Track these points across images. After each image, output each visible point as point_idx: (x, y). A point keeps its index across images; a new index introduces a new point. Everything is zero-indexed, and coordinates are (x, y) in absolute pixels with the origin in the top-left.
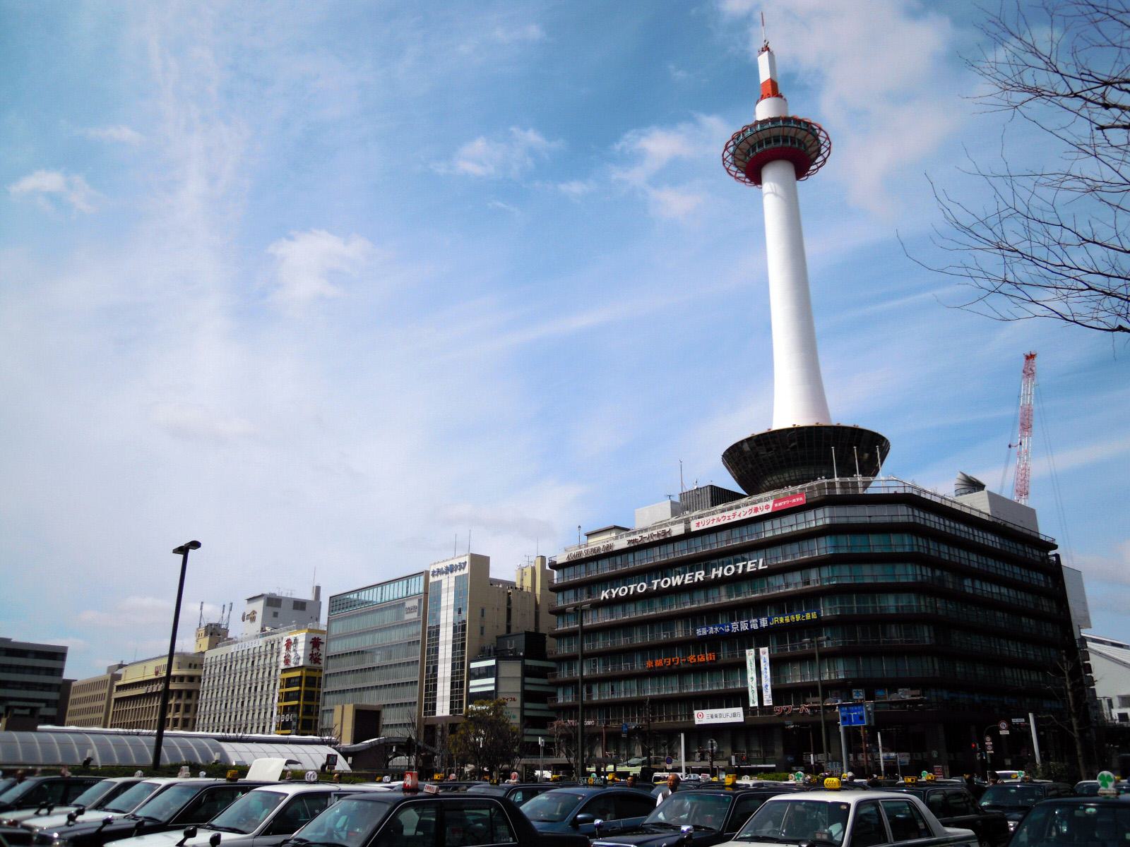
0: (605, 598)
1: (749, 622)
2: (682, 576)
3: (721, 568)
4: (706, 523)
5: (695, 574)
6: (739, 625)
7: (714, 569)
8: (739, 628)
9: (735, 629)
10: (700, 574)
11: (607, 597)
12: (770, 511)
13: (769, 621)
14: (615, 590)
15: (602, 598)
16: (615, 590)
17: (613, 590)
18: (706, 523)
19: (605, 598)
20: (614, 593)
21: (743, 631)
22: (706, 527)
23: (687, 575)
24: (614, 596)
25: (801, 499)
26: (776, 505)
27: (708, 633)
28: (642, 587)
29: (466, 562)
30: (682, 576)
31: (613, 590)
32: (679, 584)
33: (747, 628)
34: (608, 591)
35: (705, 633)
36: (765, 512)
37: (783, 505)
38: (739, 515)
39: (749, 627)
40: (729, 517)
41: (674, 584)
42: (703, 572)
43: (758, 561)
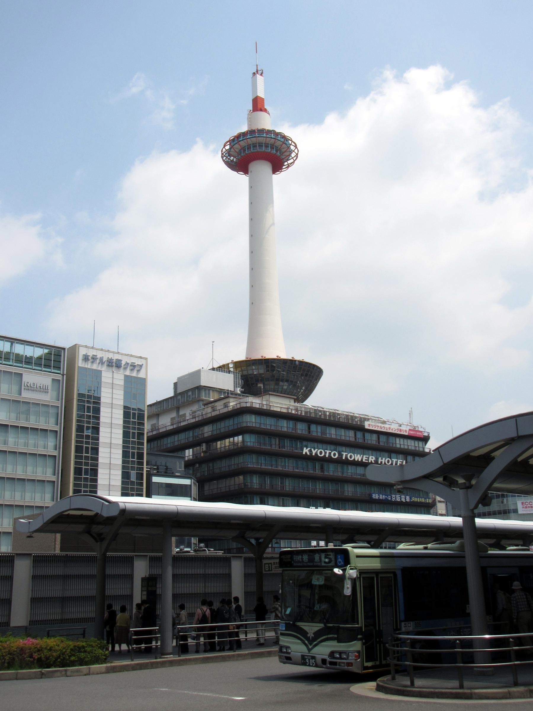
0: (306, 453)
1: (400, 497)
2: (362, 456)
3: (384, 459)
4: (374, 427)
5: (368, 458)
6: (396, 497)
7: (380, 458)
8: (396, 499)
9: (393, 499)
10: (372, 458)
11: (308, 454)
12: (407, 434)
13: (411, 498)
14: (314, 450)
15: (304, 453)
16: (314, 450)
17: (312, 449)
18: (374, 427)
19: (306, 453)
20: (314, 452)
21: (398, 502)
22: (373, 429)
23: (364, 456)
24: (314, 454)
25: (420, 434)
26: (410, 432)
27: (379, 498)
28: (335, 455)
29: (143, 364)
30: (362, 456)
31: (312, 449)
32: (360, 460)
33: (399, 500)
34: (309, 449)
35: (377, 497)
36: (405, 433)
37: (413, 434)
38: (392, 430)
39: (401, 499)
40: (387, 428)
41: (356, 460)
42: (374, 459)
43: (403, 461)
